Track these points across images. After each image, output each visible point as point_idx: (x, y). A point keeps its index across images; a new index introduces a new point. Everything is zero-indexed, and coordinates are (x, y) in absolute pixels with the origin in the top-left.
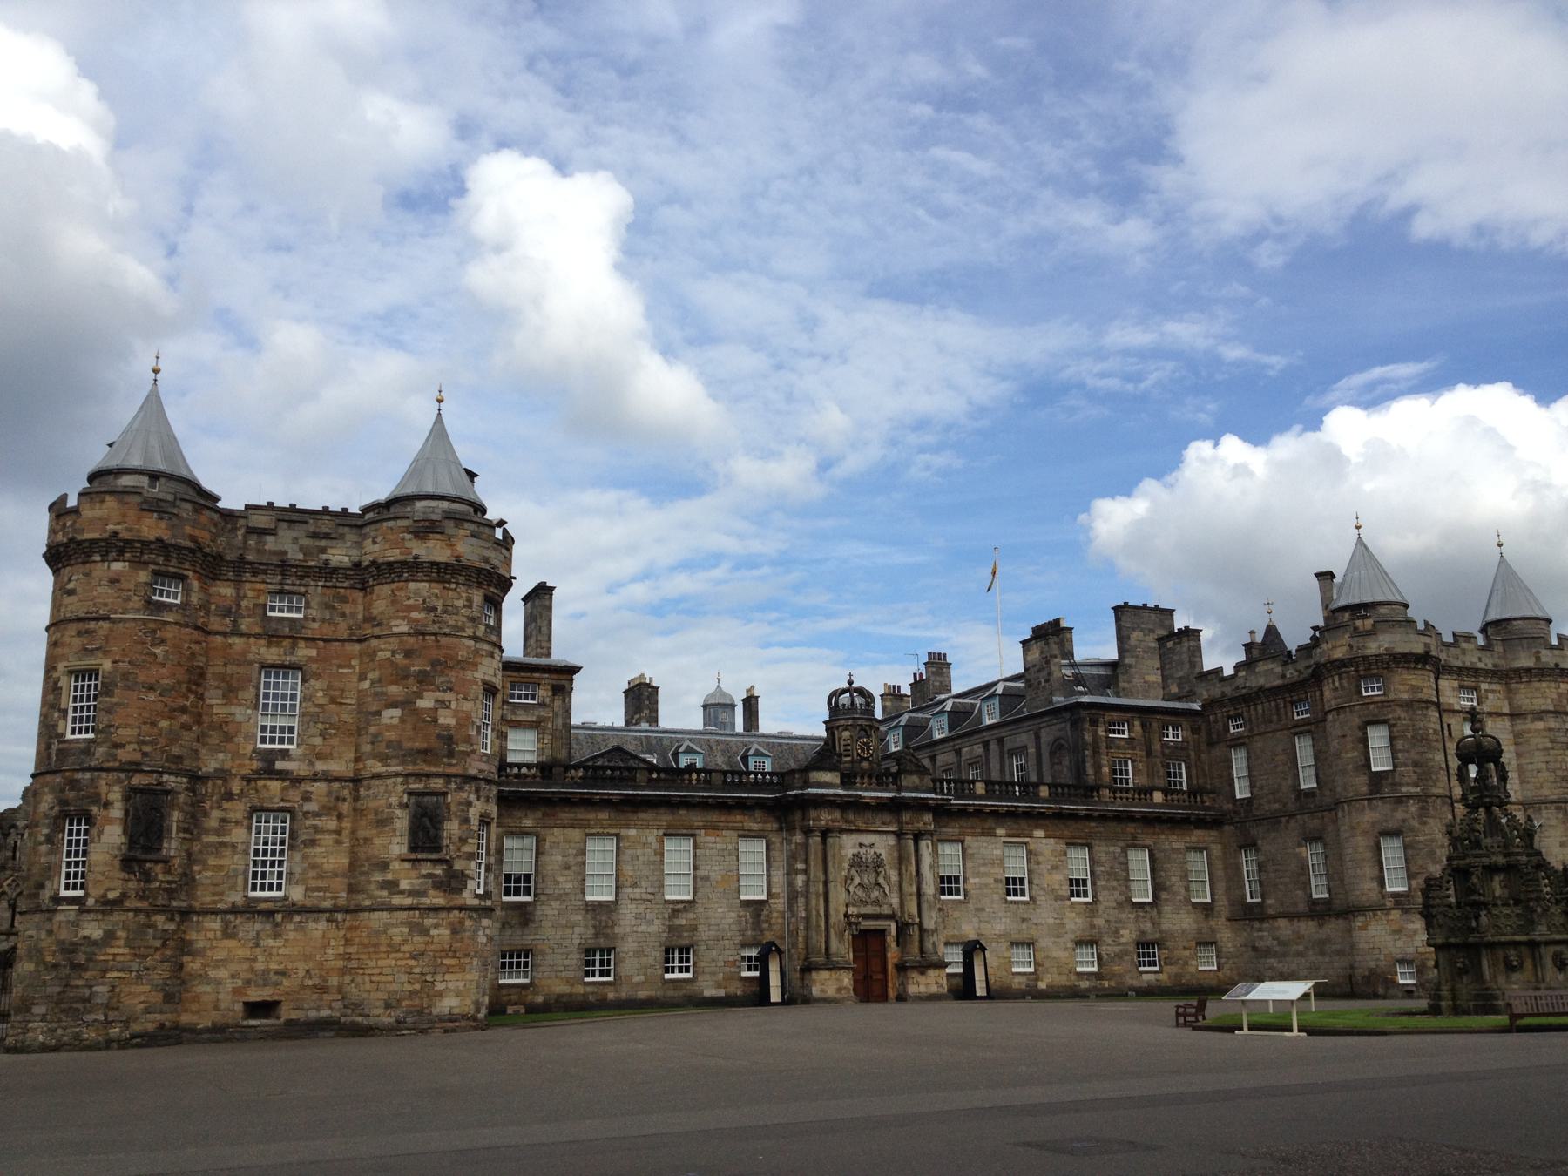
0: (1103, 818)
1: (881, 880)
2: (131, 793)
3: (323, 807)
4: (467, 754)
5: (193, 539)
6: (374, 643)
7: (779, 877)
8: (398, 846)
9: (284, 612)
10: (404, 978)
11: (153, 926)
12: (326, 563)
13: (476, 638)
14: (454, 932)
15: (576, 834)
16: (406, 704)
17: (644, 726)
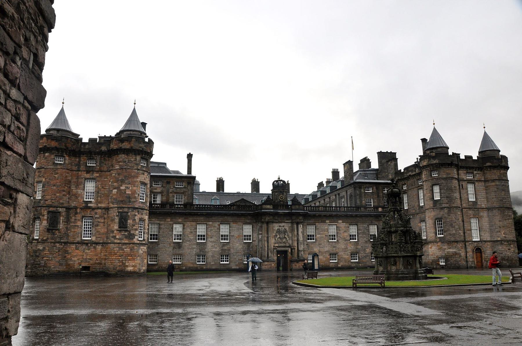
0: (361, 216)
1: (286, 236)
2: (49, 212)
3: (100, 216)
6: (112, 171)
7: (255, 235)
8: (116, 227)
9: (91, 164)
10: (118, 262)
11: (56, 246)
12: (101, 150)
14: (131, 250)
15: (194, 224)
16: (118, 188)
17: (255, 192)
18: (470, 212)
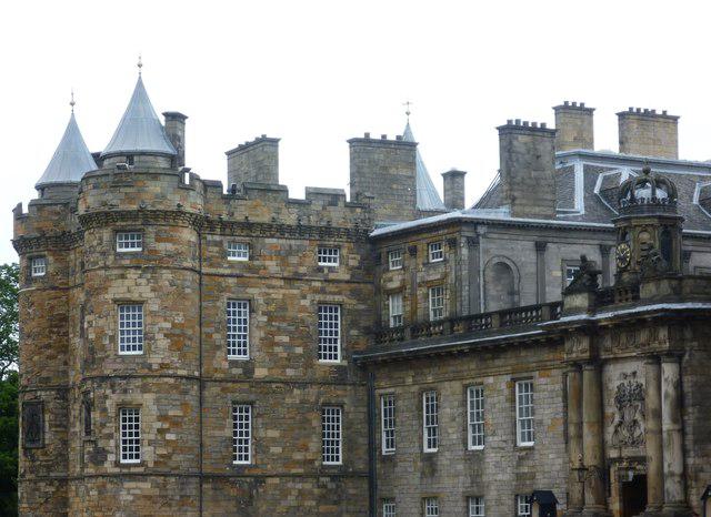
1: (638, 417)
4: (103, 359)
5: (39, 229)
13: (106, 268)
15: (457, 385)
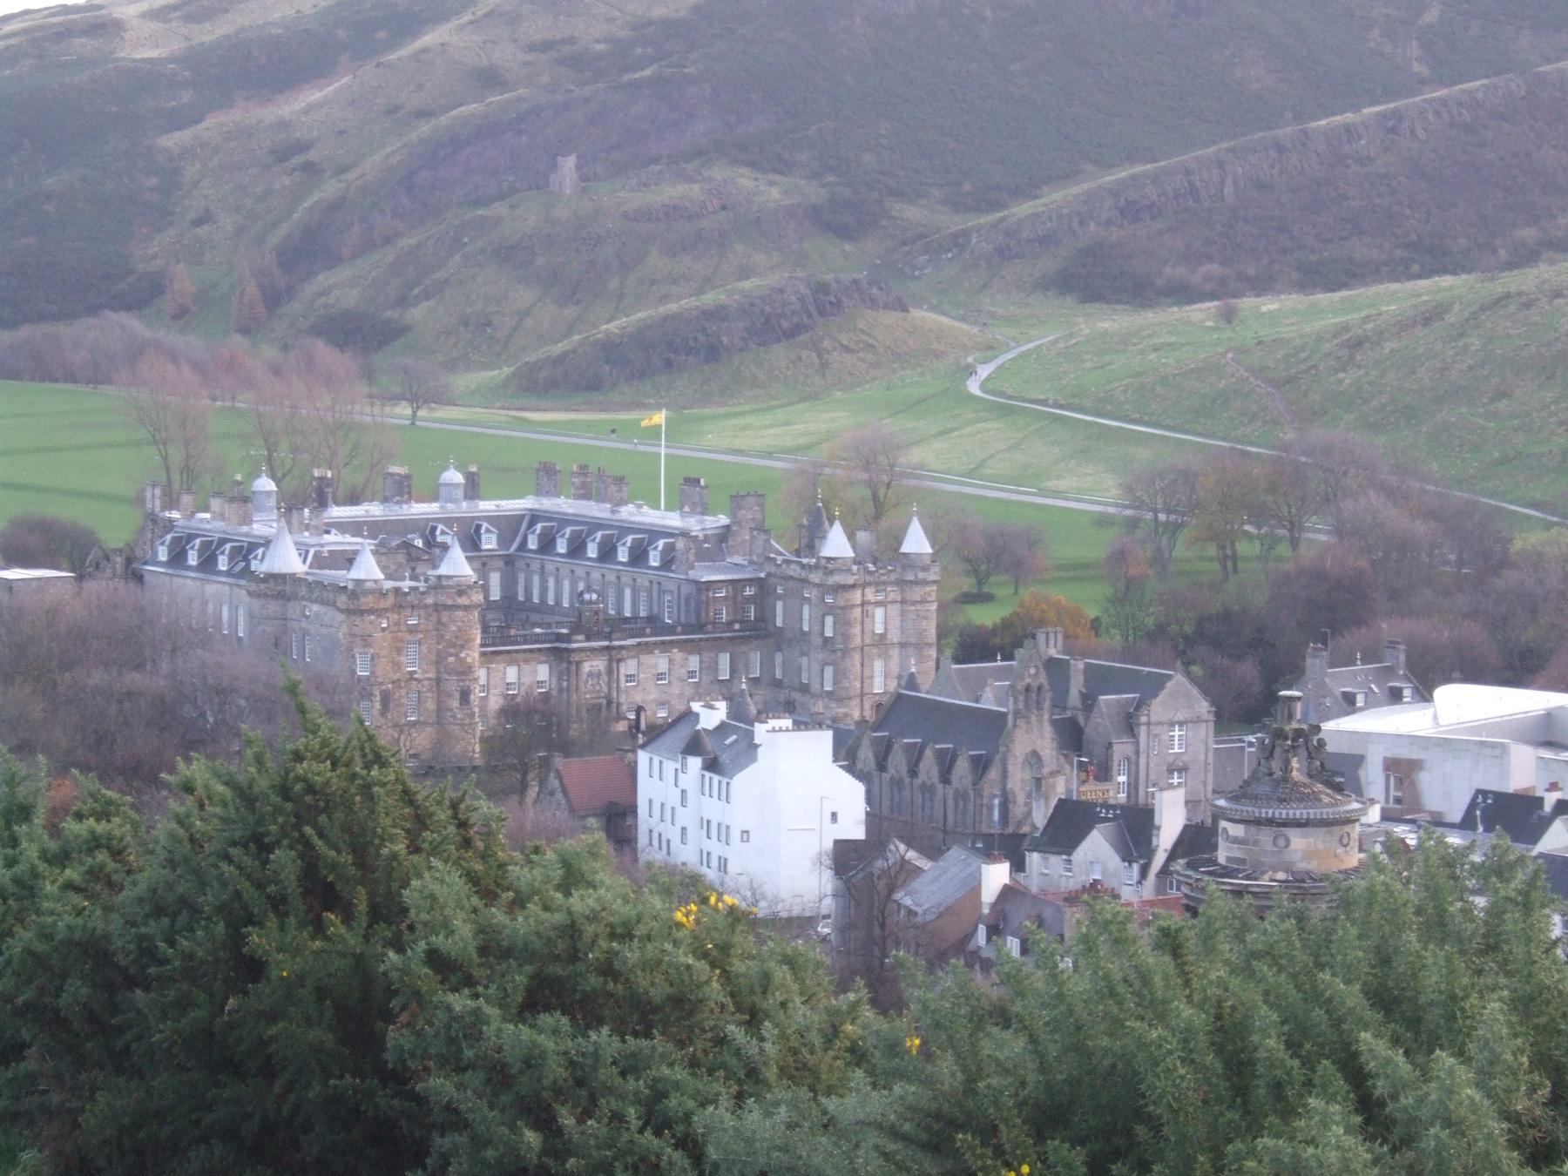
7: (554, 681)
18: (875, 651)
